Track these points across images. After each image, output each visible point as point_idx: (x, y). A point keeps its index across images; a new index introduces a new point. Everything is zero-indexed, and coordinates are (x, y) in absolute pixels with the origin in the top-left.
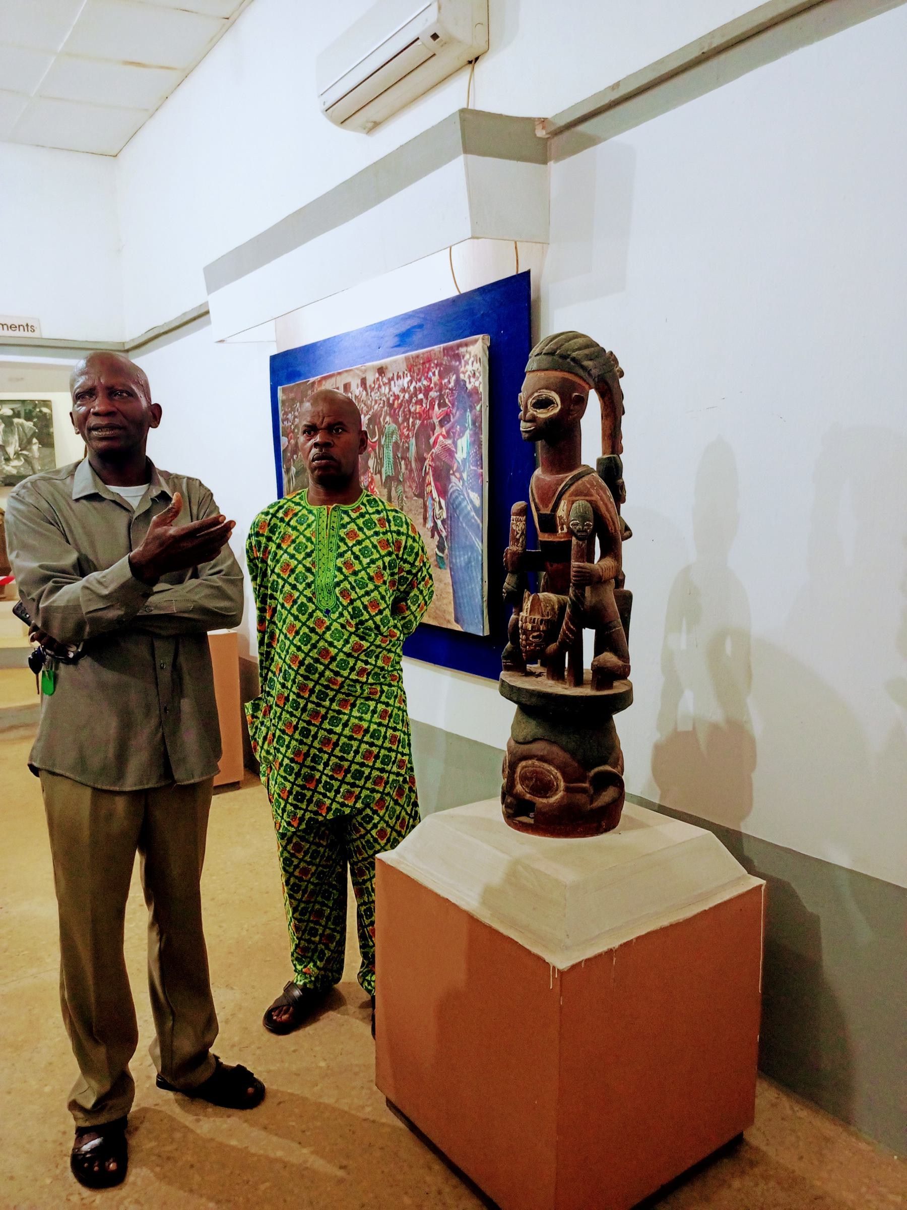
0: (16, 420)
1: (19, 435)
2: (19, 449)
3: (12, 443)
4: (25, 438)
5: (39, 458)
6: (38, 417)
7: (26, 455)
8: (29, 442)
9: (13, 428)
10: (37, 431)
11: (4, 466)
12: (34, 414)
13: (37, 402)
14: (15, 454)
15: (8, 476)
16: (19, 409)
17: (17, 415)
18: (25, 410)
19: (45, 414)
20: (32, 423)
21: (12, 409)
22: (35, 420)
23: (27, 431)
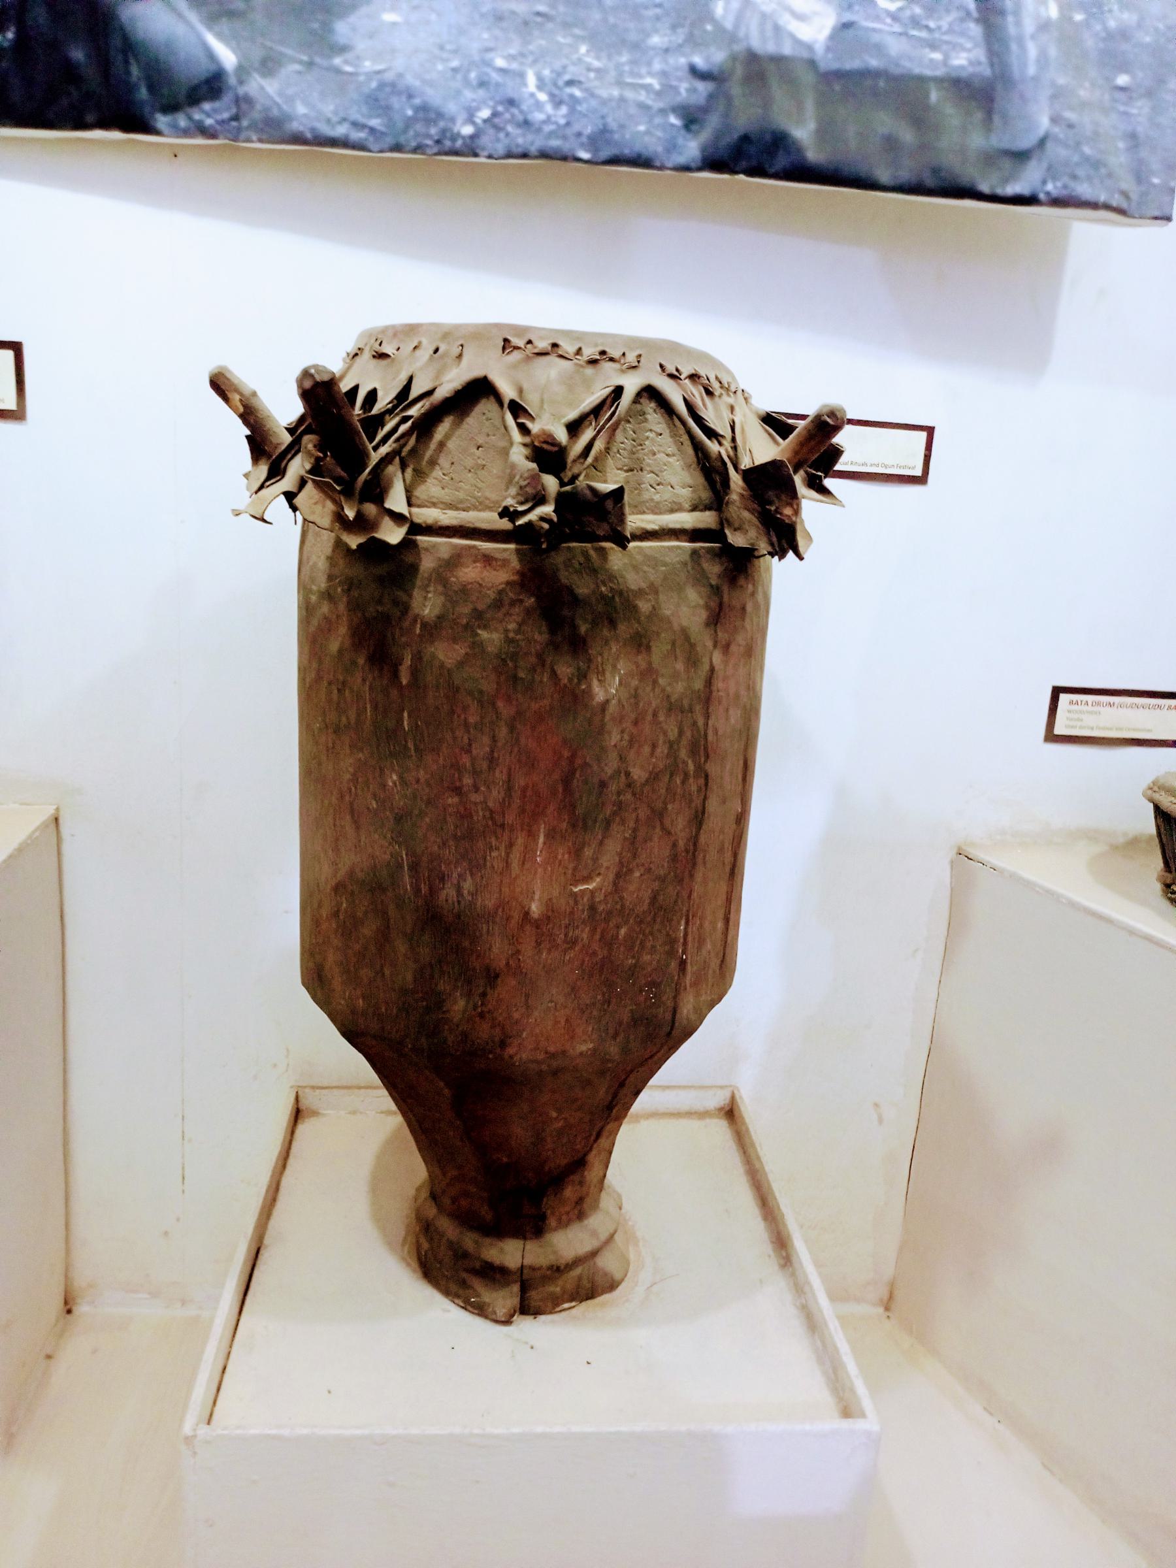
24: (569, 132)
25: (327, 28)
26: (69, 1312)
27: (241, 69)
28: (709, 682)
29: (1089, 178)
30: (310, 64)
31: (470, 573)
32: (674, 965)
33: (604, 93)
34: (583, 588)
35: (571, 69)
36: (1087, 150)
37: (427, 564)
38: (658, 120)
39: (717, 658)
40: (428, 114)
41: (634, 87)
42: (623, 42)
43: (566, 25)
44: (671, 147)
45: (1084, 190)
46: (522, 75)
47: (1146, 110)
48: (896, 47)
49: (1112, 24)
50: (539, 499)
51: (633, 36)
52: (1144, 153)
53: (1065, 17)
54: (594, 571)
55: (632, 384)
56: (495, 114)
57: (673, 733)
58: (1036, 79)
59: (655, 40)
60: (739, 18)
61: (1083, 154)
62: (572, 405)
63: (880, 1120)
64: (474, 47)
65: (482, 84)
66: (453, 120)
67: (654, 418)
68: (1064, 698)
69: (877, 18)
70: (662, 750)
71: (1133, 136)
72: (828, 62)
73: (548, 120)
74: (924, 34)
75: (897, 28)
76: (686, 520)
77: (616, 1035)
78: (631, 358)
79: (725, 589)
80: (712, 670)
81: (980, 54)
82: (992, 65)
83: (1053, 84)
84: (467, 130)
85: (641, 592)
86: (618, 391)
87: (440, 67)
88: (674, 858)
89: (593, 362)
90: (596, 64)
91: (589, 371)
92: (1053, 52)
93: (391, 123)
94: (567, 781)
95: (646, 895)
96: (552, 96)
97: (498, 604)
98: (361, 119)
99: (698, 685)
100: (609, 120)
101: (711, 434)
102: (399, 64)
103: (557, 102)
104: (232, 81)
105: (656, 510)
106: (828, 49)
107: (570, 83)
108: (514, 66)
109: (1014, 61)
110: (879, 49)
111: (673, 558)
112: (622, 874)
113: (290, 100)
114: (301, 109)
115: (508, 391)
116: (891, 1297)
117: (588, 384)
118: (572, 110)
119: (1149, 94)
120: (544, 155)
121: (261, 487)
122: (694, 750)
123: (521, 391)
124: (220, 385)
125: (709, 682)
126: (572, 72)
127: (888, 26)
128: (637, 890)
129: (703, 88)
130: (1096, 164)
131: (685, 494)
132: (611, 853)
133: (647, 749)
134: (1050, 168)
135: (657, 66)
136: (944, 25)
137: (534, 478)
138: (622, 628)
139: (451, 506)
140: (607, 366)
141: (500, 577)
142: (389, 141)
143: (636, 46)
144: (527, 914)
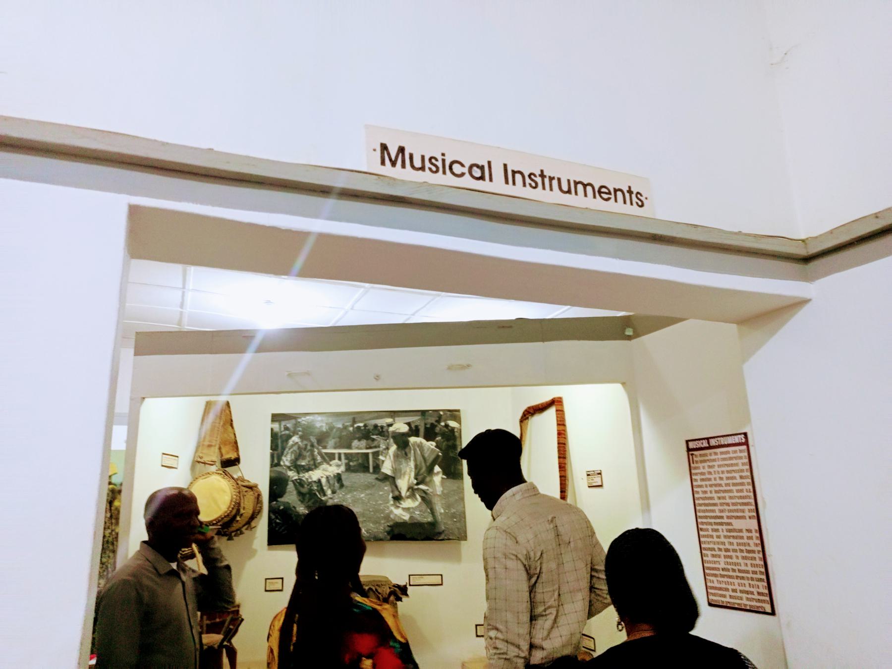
0: (412, 439)
1: (415, 460)
2: (415, 482)
3: (405, 474)
4: (423, 464)
5: (445, 496)
6: (443, 435)
7: (424, 492)
8: (430, 470)
9: (407, 450)
10: (440, 454)
11: (392, 508)
12: (437, 430)
13: (441, 413)
14: (408, 490)
15: (397, 523)
16: (417, 423)
17: (414, 432)
18: (426, 424)
20: (434, 444)
21: (409, 424)
22: (439, 438)
23: (426, 455)
43: (369, 521)
44: (385, 537)
45: (451, 537)
67: (371, 593)
72: (409, 522)
81: (432, 519)
101: (379, 593)
103: (367, 533)
110: (417, 519)
119: (459, 522)
127: (418, 516)
129: (389, 528)
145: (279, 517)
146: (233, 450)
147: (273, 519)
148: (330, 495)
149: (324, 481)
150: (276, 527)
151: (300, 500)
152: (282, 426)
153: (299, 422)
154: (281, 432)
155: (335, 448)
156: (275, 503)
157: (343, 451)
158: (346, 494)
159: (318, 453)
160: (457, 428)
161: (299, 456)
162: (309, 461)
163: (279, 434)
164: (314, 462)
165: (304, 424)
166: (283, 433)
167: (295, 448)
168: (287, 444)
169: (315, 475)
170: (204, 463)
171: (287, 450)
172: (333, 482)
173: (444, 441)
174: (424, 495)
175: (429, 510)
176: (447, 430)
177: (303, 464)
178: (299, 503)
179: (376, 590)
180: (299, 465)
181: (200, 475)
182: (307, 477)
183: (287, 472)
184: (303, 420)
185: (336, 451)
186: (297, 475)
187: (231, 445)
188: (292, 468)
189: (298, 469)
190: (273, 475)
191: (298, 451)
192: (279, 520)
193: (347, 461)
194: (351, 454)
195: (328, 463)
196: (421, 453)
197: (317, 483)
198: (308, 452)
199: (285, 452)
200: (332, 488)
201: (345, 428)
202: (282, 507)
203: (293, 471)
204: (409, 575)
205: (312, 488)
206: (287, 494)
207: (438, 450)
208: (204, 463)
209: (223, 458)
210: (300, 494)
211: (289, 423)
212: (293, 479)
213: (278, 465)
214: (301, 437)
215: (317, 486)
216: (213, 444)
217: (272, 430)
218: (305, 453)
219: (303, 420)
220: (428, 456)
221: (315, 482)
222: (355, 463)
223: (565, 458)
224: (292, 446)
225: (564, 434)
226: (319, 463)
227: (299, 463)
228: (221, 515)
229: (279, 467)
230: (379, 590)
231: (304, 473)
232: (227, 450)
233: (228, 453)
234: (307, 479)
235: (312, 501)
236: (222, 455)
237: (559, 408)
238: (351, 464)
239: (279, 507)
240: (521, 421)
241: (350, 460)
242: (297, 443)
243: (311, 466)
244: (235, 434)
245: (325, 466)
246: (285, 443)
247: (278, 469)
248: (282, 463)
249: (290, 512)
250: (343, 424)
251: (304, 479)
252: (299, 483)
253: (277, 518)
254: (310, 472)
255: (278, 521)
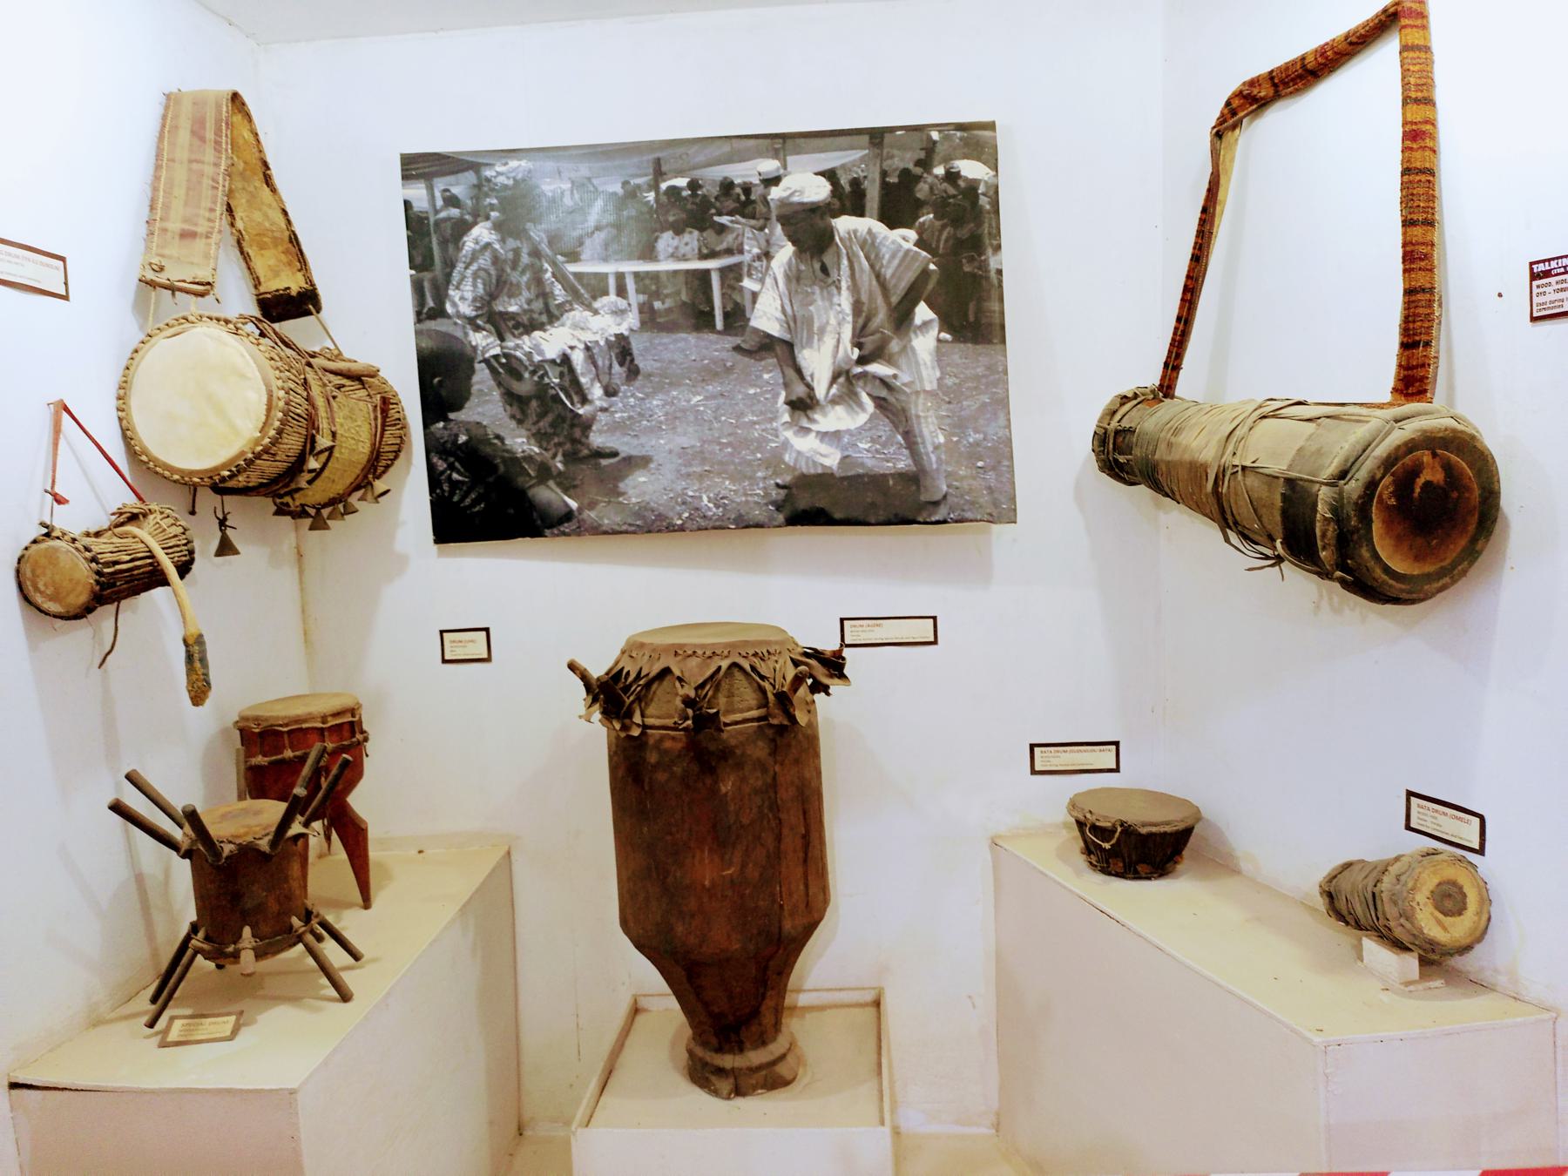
0: (844, 224)
1: (855, 288)
2: (856, 353)
3: (822, 331)
4: (880, 301)
5: (947, 395)
6: (941, 207)
7: (884, 382)
8: (902, 318)
9: (828, 258)
10: (932, 267)
11: (789, 434)
12: (922, 191)
13: (935, 135)
14: (834, 379)
15: (803, 476)
16: (858, 173)
17: (849, 199)
18: (884, 174)
19: (972, 186)
20: (912, 234)
21: (830, 175)
22: (927, 218)
23: (888, 273)
24: (725, 518)
25: (616, 487)
26: (521, 1134)
27: (580, 509)
28: (774, 778)
29: (970, 510)
30: (609, 502)
31: (668, 744)
32: (776, 906)
33: (738, 500)
34: (712, 747)
35: (723, 492)
36: (967, 498)
37: (651, 741)
38: (764, 508)
39: (777, 768)
40: (660, 517)
41: (751, 495)
42: (745, 477)
43: (719, 474)
44: (771, 519)
45: (969, 515)
46: (701, 498)
47: (994, 476)
48: (870, 463)
49: (971, 440)
50: (687, 718)
51: (749, 474)
52: (996, 495)
53: (948, 441)
54: (715, 740)
55: (725, 664)
56: (691, 514)
57: (759, 803)
58: (937, 469)
59: (760, 474)
60: (796, 460)
61: (966, 500)
62: (701, 676)
63: (974, 1006)
64: (679, 488)
65: (684, 503)
66: (672, 519)
67: (738, 674)
68: (1037, 750)
69: (860, 452)
70: (755, 810)
71: (989, 488)
72: (839, 473)
73: (714, 514)
74: (883, 456)
75: (870, 455)
76: (755, 713)
77: (751, 940)
78: (726, 653)
79: (778, 739)
80: (775, 773)
81: (910, 462)
82: (916, 465)
83: (946, 471)
84: (679, 522)
85: (736, 747)
86: (720, 667)
87: (665, 497)
88: (768, 857)
89: (710, 657)
90: (734, 488)
91: (709, 661)
92: (943, 457)
93: (645, 522)
94: (714, 826)
95: (757, 874)
96: (715, 505)
97: (679, 756)
98: (632, 522)
99: (769, 780)
100: (742, 511)
101: (763, 678)
102: (647, 498)
103: (717, 506)
104: (576, 513)
105: (742, 711)
106: (839, 468)
107: (722, 498)
108: (697, 494)
109: (926, 463)
110: (862, 465)
111: (750, 731)
112: (744, 866)
113: (601, 518)
114: (606, 521)
115: (677, 673)
116: (998, 1124)
117: (708, 666)
118: (725, 509)
119: (994, 468)
120: (715, 528)
121: (590, 706)
122: (771, 809)
123: (682, 672)
124: (572, 667)
125: (774, 778)
126: (723, 493)
127: (865, 454)
128: (753, 873)
129: (783, 492)
130: (972, 503)
131: (754, 703)
132: (737, 857)
133: (748, 811)
134: (950, 508)
135: (761, 485)
136: (891, 451)
137: (684, 711)
138: (730, 762)
139: (659, 717)
140: (716, 658)
141: (679, 745)
142: (645, 529)
143: (750, 478)
144: (704, 886)
145: (457, 464)
146: (290, 264)
147: (442, 473)
148: (600, 399)
149: (578, 358)
150: (452, 493)
151: (513, 417)
152: (438, 194)
153: (488, 180)
154: (437, 212)
155: (605, 259)
156: (441, 424)
157: (630, 267)
158: (647, 395)
159: (554, 275)
160: (986, 182)
161: (498, 286)
162: (529, 302)
163: (432, 220)
164: (546, 305)
165: (506, 187)
166: (443, 215)
167: (484, 261)
168: (459, 249)
169: (550, 343)
170: (173, 289)
171: (460, 266)
172: (607, 363)
173: (944, 227)
174: (884, 393)
175: (899, 438)
176: (952, 191)
177: (513, 309)
178: (513, 424)
179: (753, 668)
180: (501, 313)
181: (161, 325)
182: (528, 350)
183: (466, 334)
184: (499, 174)
185: (609, 268)
186: (499, 342)
187: (280, 248)
188: (479, 322)
189: (500, 324)
190: (427, 344)
191: (493, 272)
192: (459, 472)
193: (642, 298)
194: (655, 276)
195: (589, 307)
196: (872, 266)
197: (559, 365)
198: (523, 272)
199: (456, 276)
200: (605, 379)
201: (632, 194)
202: (463, 438)
203: (485, 333)
204: (842, 620)
205: (546, 380)
206: (473, 401)
207: (924, 254)
208: (173, 289)
209: (262, 289)
210: (511, 397)
211: (457, 184)
212: (487, 355)
213: (439, 313)
214: (498, 227)
215: (561, 375)
216: (199, 230)
217: (407, 204)
218: (514, 277)
219: (500, 173)
220: (893, 275)
221: (553, 362)
222: (669, 303)
223: (1430, 223)
224: (474, 256)
225: (1433, 137)
226: (560, 306)
227: (499, 307)
228: (243, 453)
229: (439, 320)
230: (764, 669)
231: (519, 337)
232: (272, 262)
233: (276, 274)
234: (529, 355)
235: (550, 418)
236: (257, 283)
237: (1414, 37)
238: (657, 305)
239: (457, 436)
240: (1218, 135)
241: (657, 295)
242: (488, 245)
243: (536, 316)
244: (285, 213)
245: (578, 314)
246: (451, 248)
247: (439, 325)
248: (449, 309)
249: (488, 450)
250: (625, 183)
251: (518, 354)
252: (507, 368)
253: (451, 467)
254: (537, 334)
255: (455, 476)
